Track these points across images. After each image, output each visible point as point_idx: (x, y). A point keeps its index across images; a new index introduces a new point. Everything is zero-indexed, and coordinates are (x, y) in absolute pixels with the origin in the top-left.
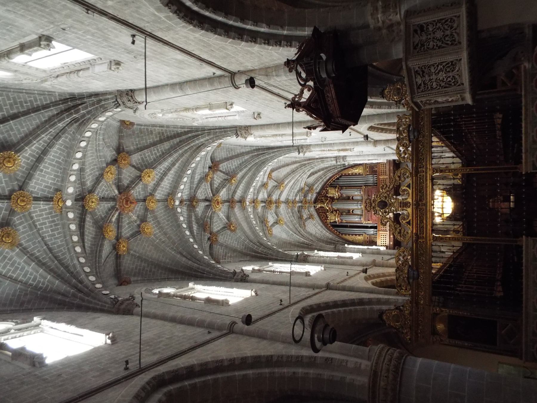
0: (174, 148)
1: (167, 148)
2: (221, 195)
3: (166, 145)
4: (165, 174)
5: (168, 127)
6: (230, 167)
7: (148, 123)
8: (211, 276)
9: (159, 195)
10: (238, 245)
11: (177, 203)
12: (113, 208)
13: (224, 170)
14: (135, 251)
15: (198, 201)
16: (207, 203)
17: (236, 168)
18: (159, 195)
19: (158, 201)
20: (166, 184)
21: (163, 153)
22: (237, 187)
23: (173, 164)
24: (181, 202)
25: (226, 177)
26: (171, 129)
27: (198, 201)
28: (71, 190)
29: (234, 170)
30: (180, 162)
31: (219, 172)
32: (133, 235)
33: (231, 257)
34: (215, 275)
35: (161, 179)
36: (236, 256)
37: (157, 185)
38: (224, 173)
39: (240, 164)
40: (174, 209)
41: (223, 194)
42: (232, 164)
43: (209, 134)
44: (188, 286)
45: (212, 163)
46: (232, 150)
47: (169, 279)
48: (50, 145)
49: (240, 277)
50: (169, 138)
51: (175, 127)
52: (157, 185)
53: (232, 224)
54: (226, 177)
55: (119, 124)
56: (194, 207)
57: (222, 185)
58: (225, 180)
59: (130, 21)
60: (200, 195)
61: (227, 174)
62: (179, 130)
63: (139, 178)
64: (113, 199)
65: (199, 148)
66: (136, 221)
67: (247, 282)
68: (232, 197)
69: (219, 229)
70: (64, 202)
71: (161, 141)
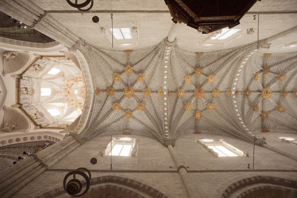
0: (225, 62)
1: (222, 62)
2: (271, 87)
3: (222, 61)
4: (223, 77)
5: (221, 51)
6: (280, 69)
7: (210, 51)
8: (243, 138)
9: (221, 88)
10: (286, 121)
11: (233, 93)
12: (193, 96)
13: (275, 71)
14: (205, 118)
15: (250, 92)
16: (259, 93)
17: (285, 69)
18: (221, 88)
19: (221, 92)
20: (225, 82)
21: (220, 66)
22: (288, 81)
23: (228, 71)
24: (237, 92)
25: (276, 76)
26: (223, 52)
27: (250, 92)
28: (165, 88)
29: (283, 70)
30: (232, 69)
31: (269, 73)
32: (204, 110)
33: (279, 129)
34: (245, 138)
35: (221, 80)
36: (284, 129)
37: (220, 83)
38: (275, 73)
39: (289, 66)
40: (231, 96)
41: (274, 86)
42: (282, 67)
43: (243, 50)
44: (219, 141)
45: (263, 67)
46: (281, 57)
47: (221, 135)
48: (155, 69)
49: (258, 142)
50: (223, 57)
51: (224, 50)
52: (220, 83)
53: (280, 107)
54: (276, 76)
55: (195, 55)
56: (247, 95)
57: (273, 81)
58: (276, 77)
59: (99, 10)
60: (252, 88)
61: (278, 74)
62: (228, 51)
63: (207, 80)
64: (193, 91)
65: (242, 58)
66: (205, 103)
67: (263, 147)
68: (283, 89)
69: (270, 109)
70: (163, 93)
71: (219, 59)
